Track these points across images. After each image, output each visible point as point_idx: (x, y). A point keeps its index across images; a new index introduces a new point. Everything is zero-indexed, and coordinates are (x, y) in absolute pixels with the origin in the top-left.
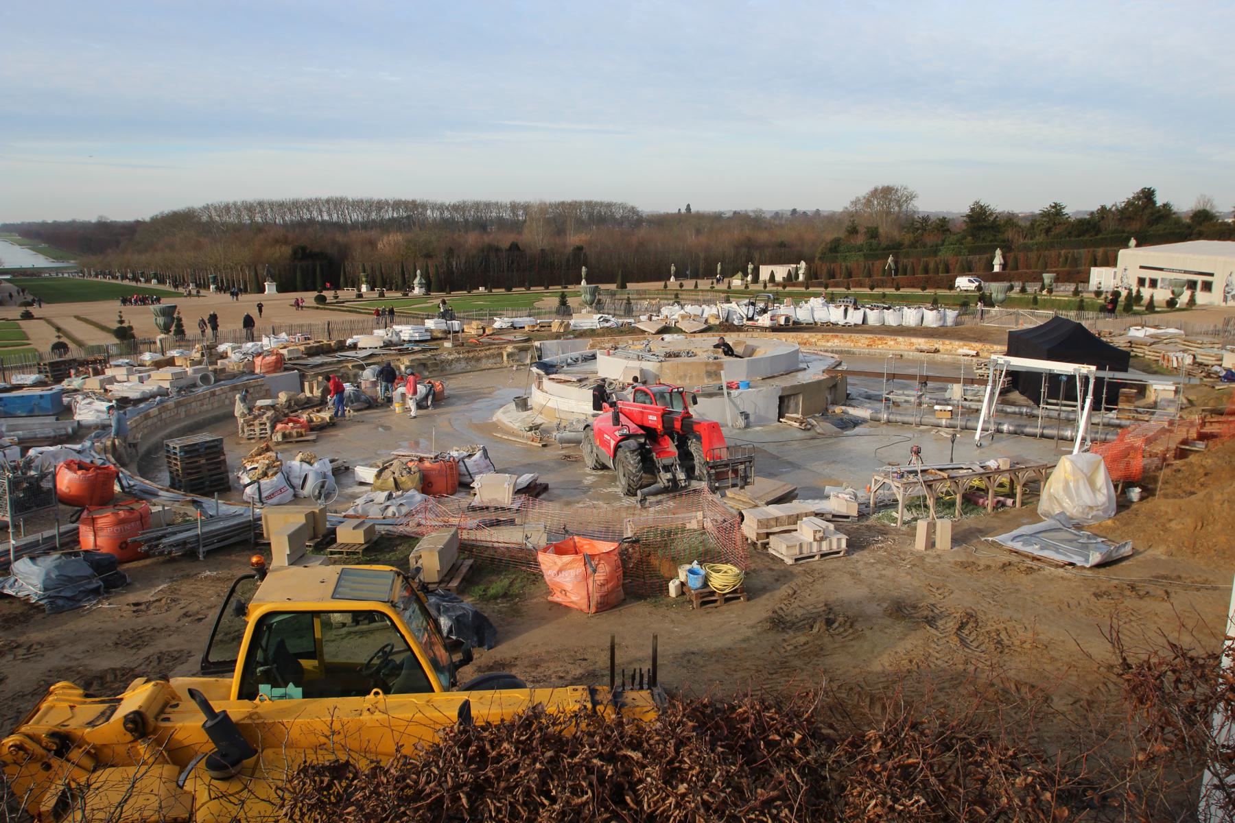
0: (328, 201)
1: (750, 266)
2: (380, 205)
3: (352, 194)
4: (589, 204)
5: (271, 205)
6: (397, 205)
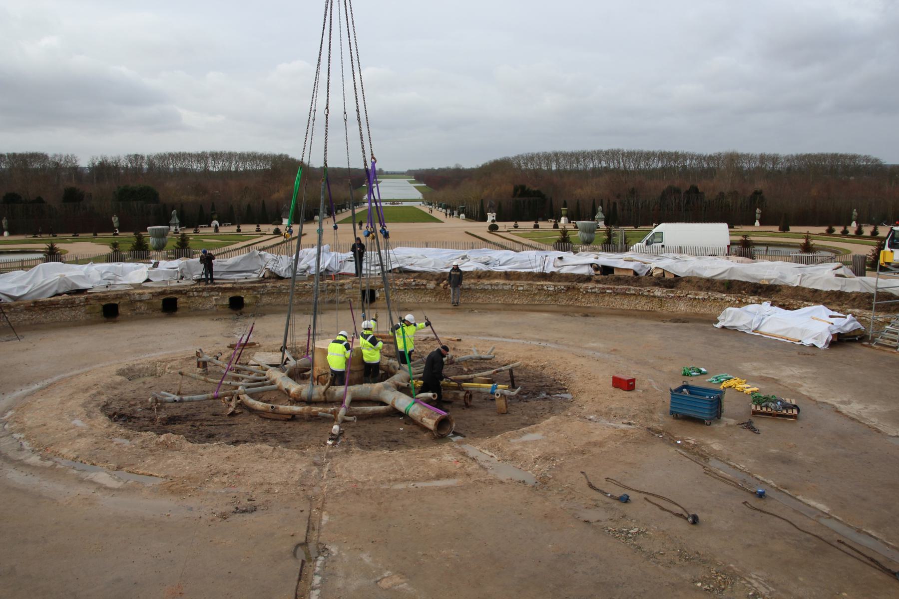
0: (607, 153)
2: (648, 156)
4: (835, 157)
5: (565, 155)
6: (663, 156)
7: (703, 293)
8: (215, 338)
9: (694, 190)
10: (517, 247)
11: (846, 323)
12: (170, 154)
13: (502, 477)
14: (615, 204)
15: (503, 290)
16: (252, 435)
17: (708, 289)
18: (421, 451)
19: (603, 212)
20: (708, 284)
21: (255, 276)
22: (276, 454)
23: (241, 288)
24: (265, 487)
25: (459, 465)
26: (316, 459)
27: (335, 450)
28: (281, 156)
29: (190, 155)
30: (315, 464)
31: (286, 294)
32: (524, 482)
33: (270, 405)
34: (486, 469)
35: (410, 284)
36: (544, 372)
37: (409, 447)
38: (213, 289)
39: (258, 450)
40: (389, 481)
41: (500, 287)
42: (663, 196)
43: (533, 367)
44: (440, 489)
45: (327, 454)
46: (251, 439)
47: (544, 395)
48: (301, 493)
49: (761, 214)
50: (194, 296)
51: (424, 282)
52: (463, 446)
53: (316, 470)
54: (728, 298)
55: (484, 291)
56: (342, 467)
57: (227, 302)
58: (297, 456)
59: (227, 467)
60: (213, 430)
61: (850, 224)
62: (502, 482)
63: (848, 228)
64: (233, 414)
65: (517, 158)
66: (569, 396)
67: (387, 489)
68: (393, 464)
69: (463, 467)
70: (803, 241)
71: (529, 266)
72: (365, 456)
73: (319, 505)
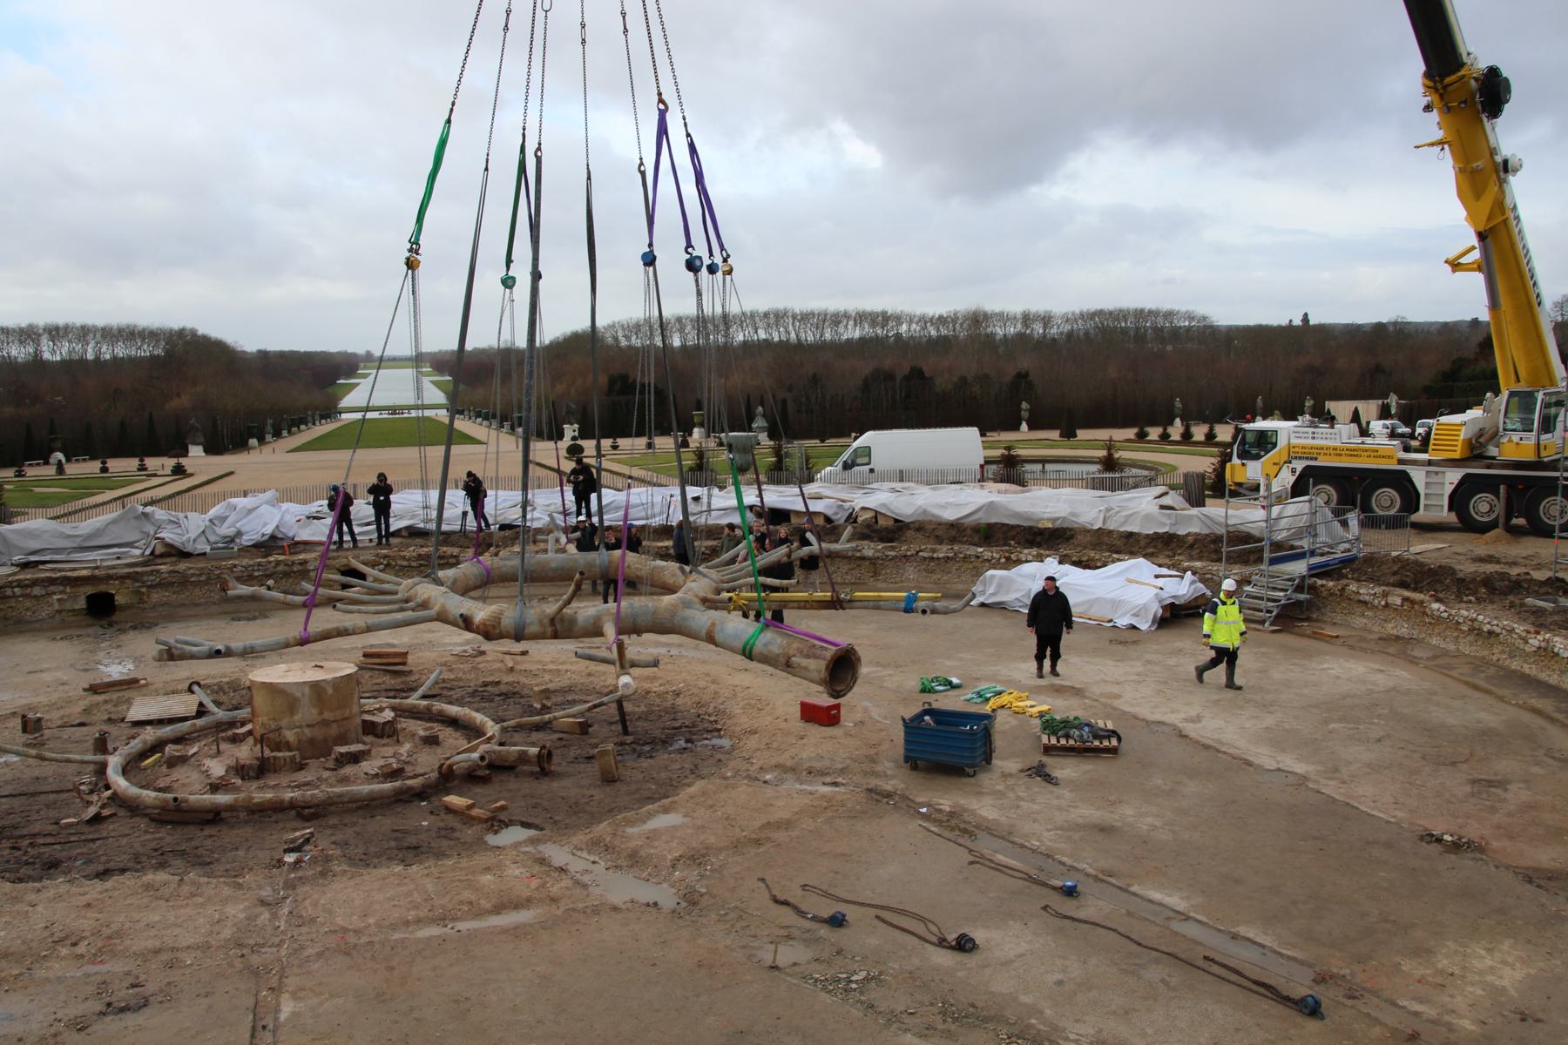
0: (766, 315)
1: (1309, 403)
2: (837, 319)
3: (799, 305)
4: (1140, 314)
6: (861, 318)
7: (945, 548)
8: (59, 674)
9: (917, 373)
10: (620, 482)
11: (1182, 587)
13: (616, 898)
14: (784, 402)
16: (137, 858)
17: (953, 540)
18: (464, 863)
19: (764, 416)
20: (953, 532)
21: (137, 552)
22: (185, 889)
23: (110, 577)
24: (165, 957)
25: (535, 883)
26: (266, 893)
27: (300, 874)
28: (181, 332)
30: (263, 903)
31: (198, 584)
32: (656, 904)
33: (170, 796)
34: (585, 886)
35: (427, 557)
36: (679, 701)
37: (440, 855)
38: (52, 581)
39: (148, 887)
40: (407, 923)
42: (866, 386)
43: (659, 695)
44: (504, 931)
45: (285, 883)
46: (136, 864)
47: (682, 743)
48: (238, 963)
49: (1031, 411)
50: (14, 596)
51: (455, 551)
52: (541, 848)
53: (266, 915)
54: (988, 555)
56: (315, 905)
57: (82, 603)
58: (227, 891)
59: (86, 923)
60: (57, 851)
61: (1171, 423)
62: (615, 909)
63: (1170, 430)
64: (97, 819)
65: (613, 326)
66: (725, 742)
67: (403, 940)
68: (410, 894)
69: (543, 886)
70: (1103, 453)
71: (643, 514)
72: (358, 880)
73: (274, 982)
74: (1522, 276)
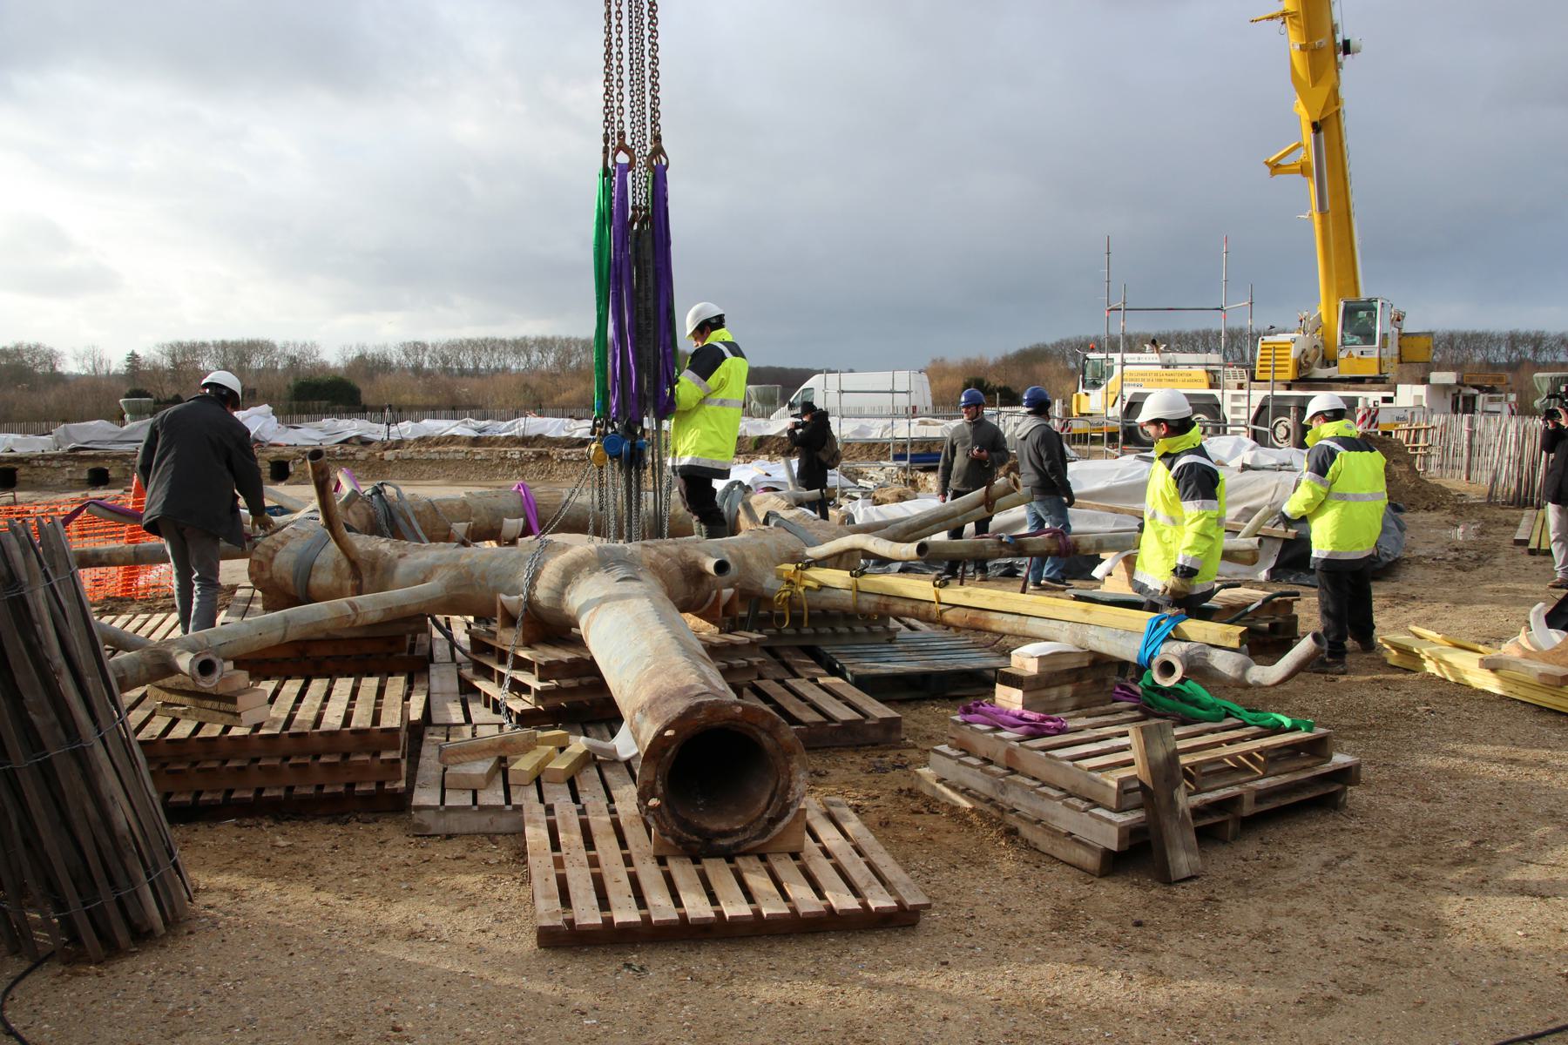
12: (469, 342)
15: (455, 460)
29: (504, 343)
41: (451, 456)
55: (431, 461)
57: (85, 475)
74: (1345, 179)
